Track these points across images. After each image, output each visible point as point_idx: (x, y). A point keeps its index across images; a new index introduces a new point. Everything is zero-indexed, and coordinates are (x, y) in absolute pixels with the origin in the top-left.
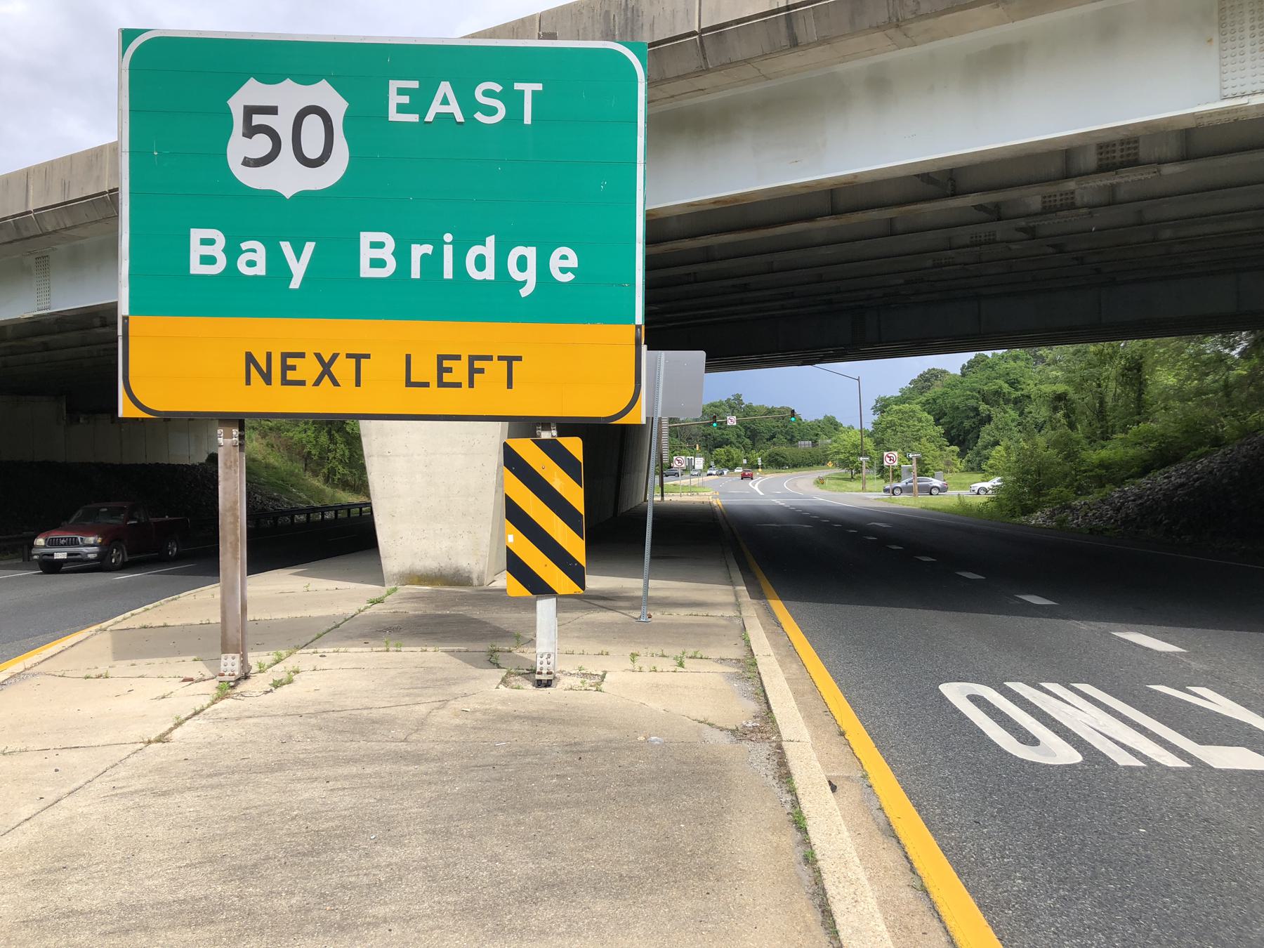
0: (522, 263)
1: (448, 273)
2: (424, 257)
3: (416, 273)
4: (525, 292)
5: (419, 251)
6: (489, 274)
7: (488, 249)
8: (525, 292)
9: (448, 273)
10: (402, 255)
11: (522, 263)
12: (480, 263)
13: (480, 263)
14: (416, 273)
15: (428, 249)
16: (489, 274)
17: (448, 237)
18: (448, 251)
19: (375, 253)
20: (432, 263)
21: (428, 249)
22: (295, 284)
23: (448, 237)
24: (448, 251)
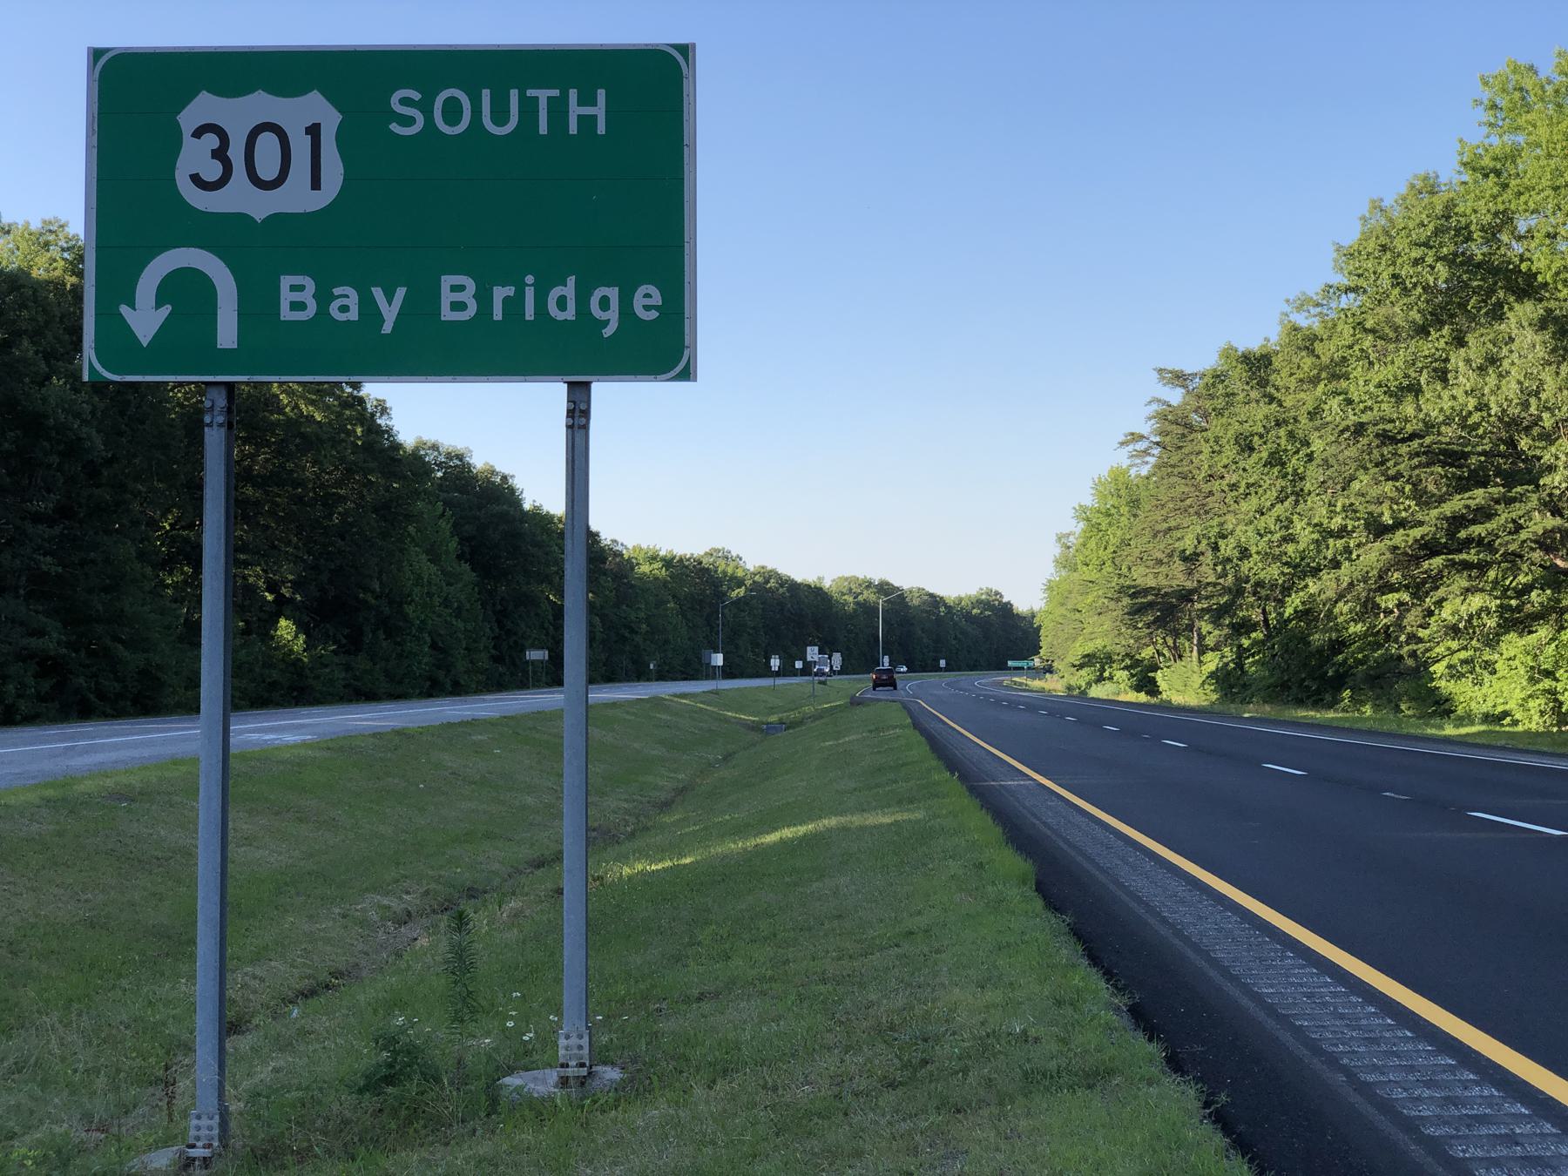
0: (605, 303)
1: (530, 314)
2: (506, 300)
3: (498, 314)
4: (608, 332)
5: (500, 293)
6: (570, 314)
7: (569, 289)
8: (608, 332)
9: (530, 314)
10: (484, 298)
11: (605, 303)
12: (562, 303)
13: (562, 303)
14: (498, 314)
15: (510, 291)
16: (570, 314)
17: (530, 279)
18: (530, 293)
19: (457, 296)
20: (513, 305)
21: (510, 291)
22: (387, 328)
23: (530, 279)
24: (530, 293)
